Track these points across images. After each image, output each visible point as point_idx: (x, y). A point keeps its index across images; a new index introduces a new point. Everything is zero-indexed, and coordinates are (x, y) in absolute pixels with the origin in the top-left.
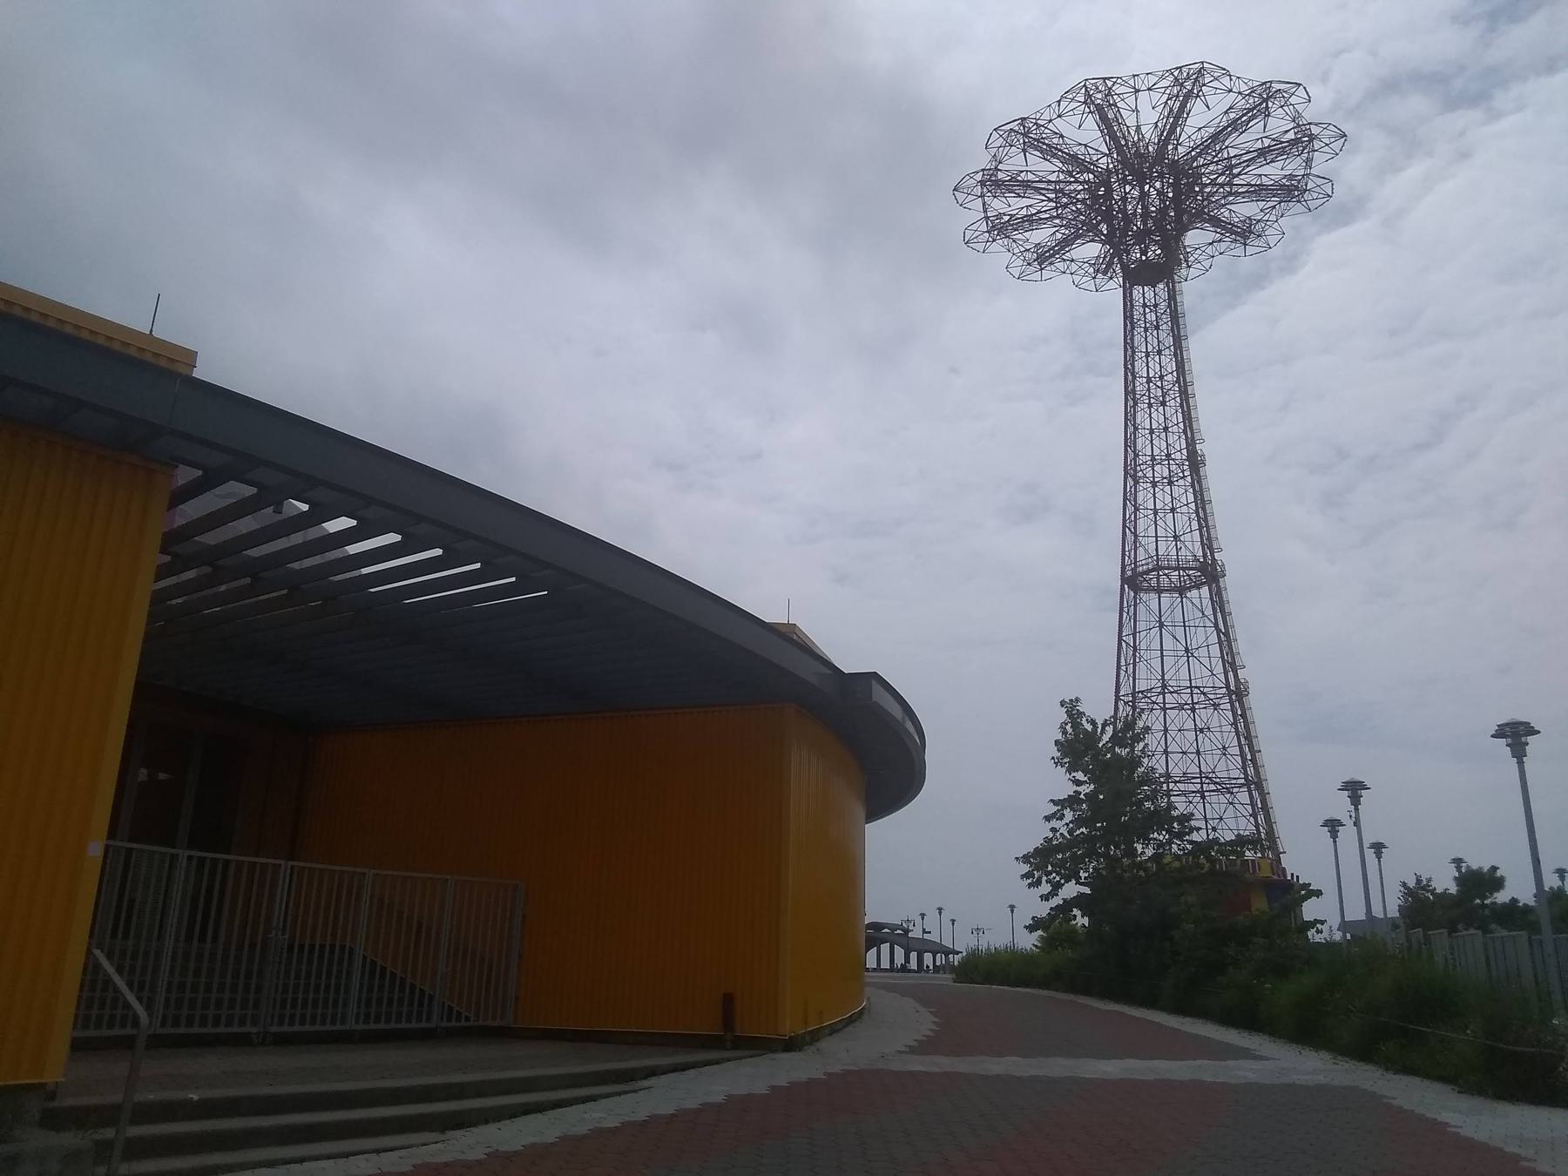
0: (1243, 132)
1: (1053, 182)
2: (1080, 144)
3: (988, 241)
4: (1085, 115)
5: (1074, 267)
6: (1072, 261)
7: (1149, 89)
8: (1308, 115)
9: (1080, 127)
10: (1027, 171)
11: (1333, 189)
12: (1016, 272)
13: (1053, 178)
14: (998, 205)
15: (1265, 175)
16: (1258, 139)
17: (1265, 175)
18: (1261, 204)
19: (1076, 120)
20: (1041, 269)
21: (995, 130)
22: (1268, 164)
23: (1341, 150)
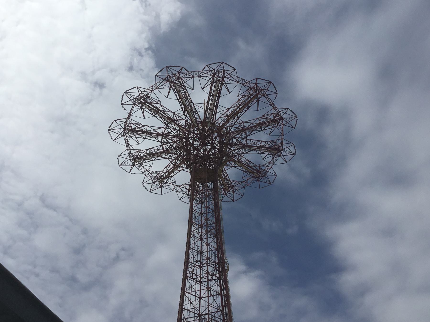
0: (262, 130)
5: (147, 173)
7: (243, 84)
12: (121, 160)
16: (260, 141)
18: (245, 174)
20: (134, 165)
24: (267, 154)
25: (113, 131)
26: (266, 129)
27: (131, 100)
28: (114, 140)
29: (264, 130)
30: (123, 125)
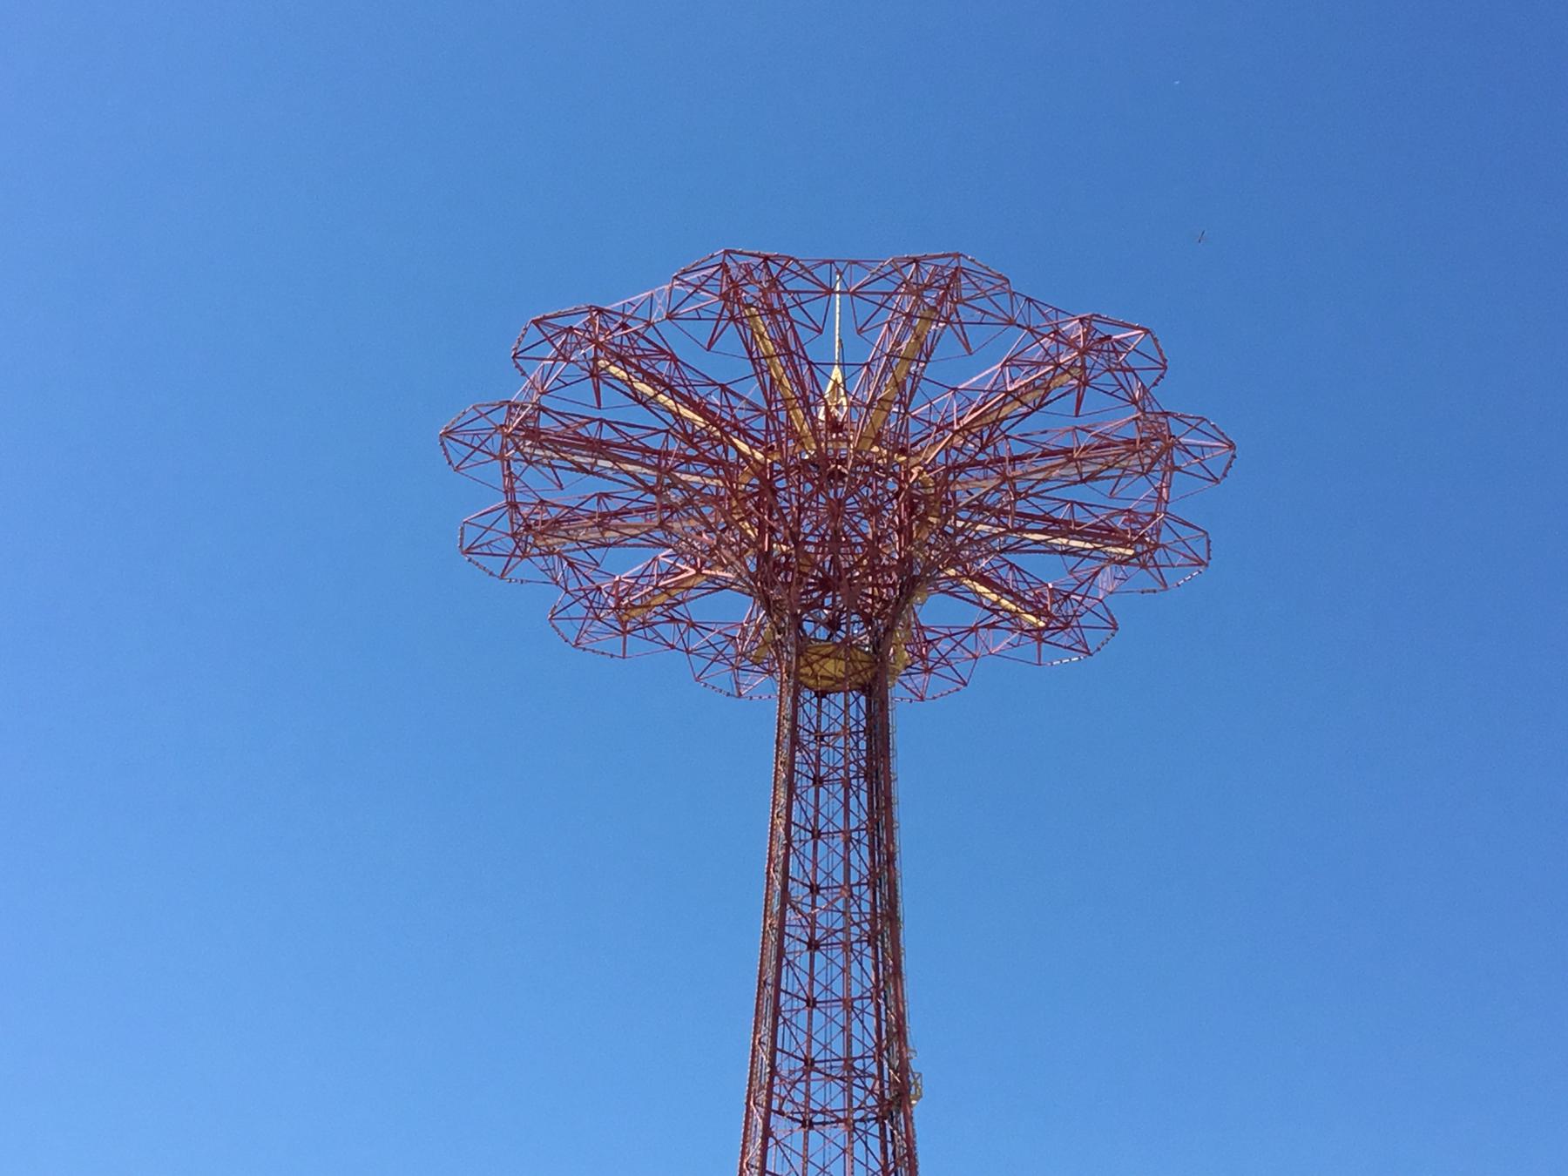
1: (655, 452)
2: (714, 384)
3: (513, 555)
4: (722, 324)
6: (693, 625)
8: (1165, 397)
9: (711, 344)
10: (602, 421)
11: (1209, 550)
13: (655, 442)
14: (535, 481)
15: (1081, 504)
17: (1081, 504)
19: (704, 331)
21: (536, 322)
22: (1083, 481)
23: (1225, 475)
24: (1120, 477)
25: (478, 550)
26: (1045, 401)
27: (478, 449)
28: (502, 576)
29: (1040, 406)
30: (504, 525)
